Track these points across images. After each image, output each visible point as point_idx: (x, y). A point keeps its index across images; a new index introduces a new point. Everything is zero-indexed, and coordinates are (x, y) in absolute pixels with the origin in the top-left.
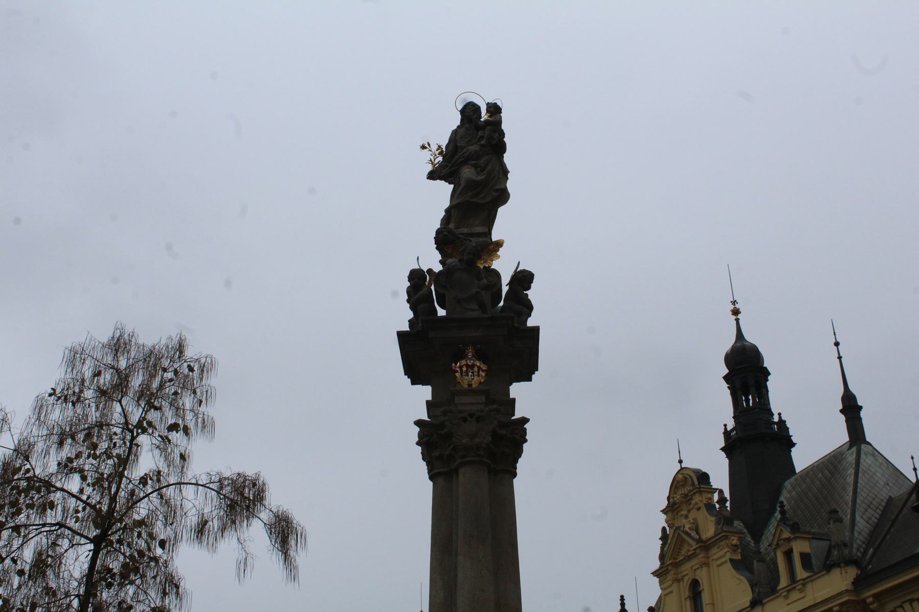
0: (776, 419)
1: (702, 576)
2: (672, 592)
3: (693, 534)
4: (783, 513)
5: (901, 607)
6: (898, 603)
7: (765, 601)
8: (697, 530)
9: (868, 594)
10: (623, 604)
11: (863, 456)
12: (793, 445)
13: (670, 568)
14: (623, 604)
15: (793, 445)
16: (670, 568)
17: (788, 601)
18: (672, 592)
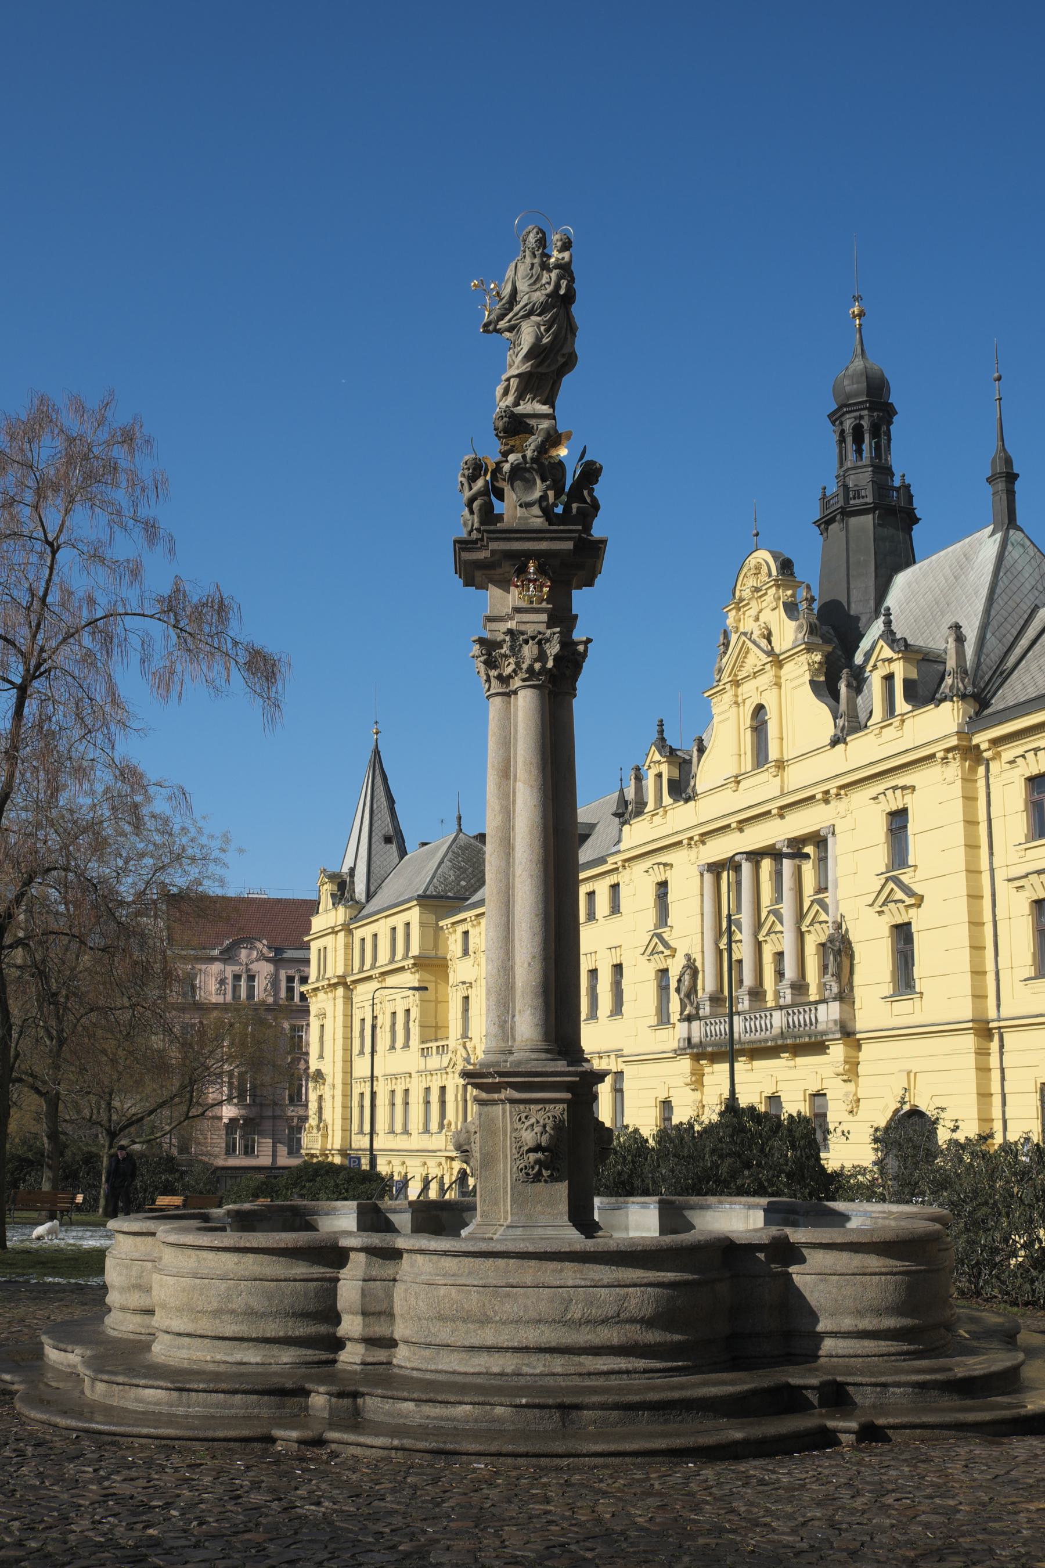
0: (897, 483)
1: (769, 700)
2: (728, 719)
3: (764, 643)
4: (888, 623)
5: (1023, 756)
6: (1020, 751)
7: (848, 739)
8: (768, 637)
9: (982, 739)
10: (661, 732)
11: (1009, 548)
12: (917, 520)
13: (728, 686)
14: (661, 732)
15: (917, 520)
16: (728, 686)
17: (881, 741)
18: (728, 719)
